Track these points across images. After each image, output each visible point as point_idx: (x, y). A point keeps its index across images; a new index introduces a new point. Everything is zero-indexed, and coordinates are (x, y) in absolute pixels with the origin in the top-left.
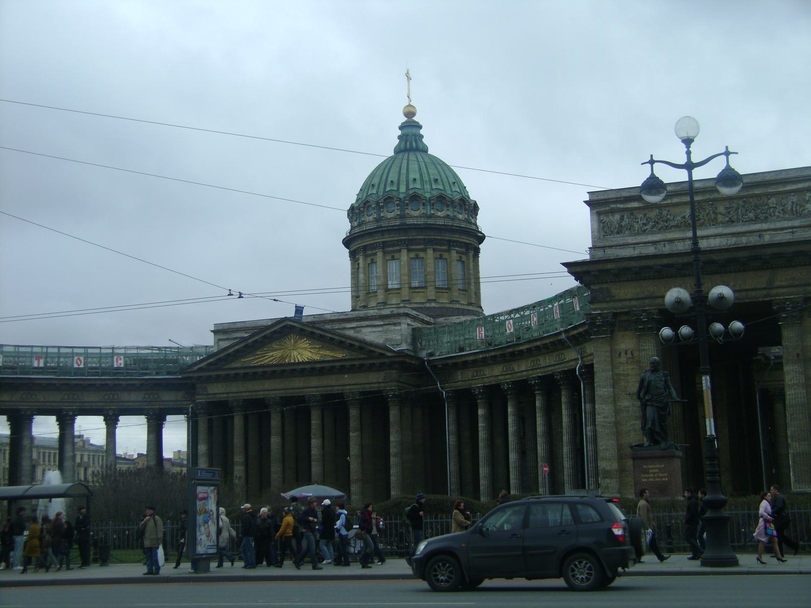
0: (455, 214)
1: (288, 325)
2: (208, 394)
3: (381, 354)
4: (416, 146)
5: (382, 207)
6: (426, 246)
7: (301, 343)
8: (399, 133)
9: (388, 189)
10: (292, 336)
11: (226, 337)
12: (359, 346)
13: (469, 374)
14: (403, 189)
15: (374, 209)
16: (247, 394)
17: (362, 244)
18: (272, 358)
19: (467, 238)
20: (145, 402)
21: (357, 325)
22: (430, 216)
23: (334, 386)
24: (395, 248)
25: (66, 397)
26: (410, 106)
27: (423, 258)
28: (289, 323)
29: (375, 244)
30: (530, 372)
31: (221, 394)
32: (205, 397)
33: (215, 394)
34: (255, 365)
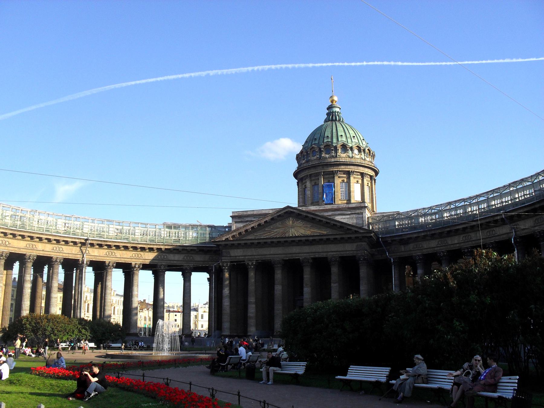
0: (366, 157)
1: (289, 211)
2: (231, 256)
3: (355, 231)
5: (322, 151)
8: (327, 111)
9: (325, 141)
10: (291, 219)
11: (240, 221)
13: (411, 246)
14: (335, 140)
16: (258, 257)
17: (309, 173)
18: (276, 233)
19: (371, 172)
20: (184, 261)
21: (332, 213)
23: (320, 252)
24: (331, 176)
25: (134, 255)
28: (290, 210)
29: (318, 173)
30: (462, 244)
31: (240, 256)
32: (229, 258)
33: (236, 256)
34: (264, 237)
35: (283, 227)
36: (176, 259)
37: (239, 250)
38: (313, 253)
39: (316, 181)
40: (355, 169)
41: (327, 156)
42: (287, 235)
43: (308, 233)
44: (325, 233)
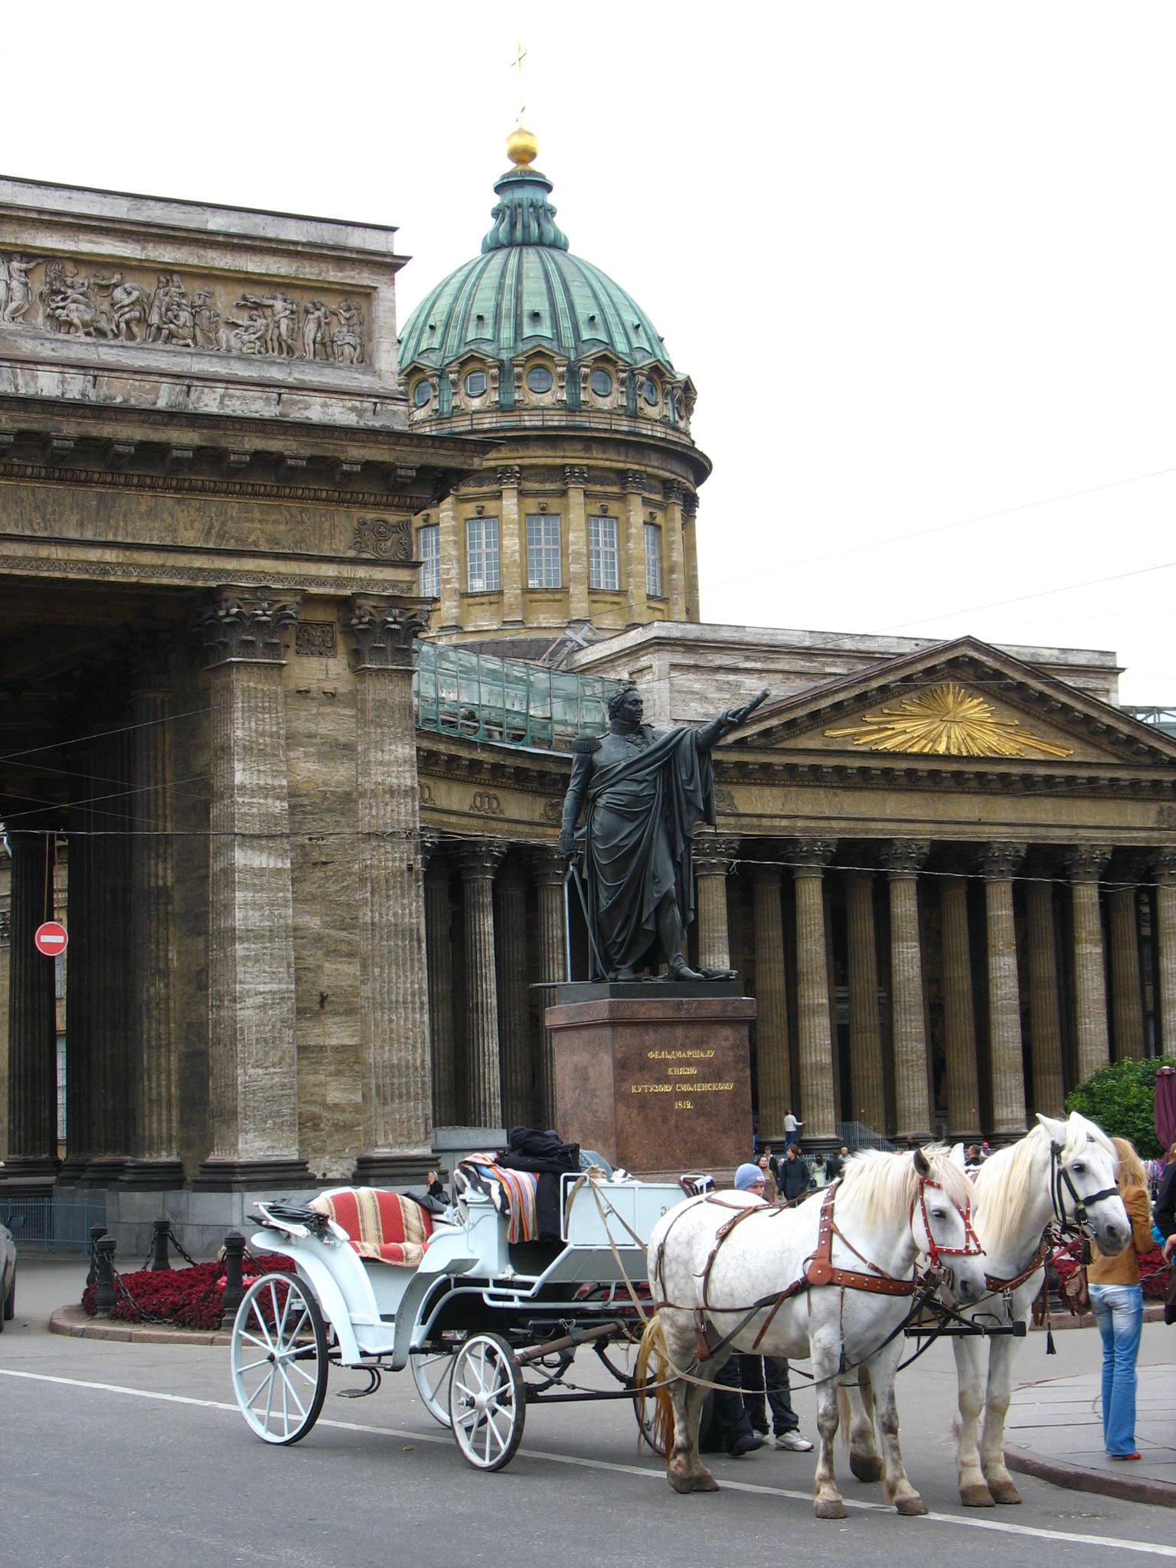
1: (964, 656)
4: (541, 234)
5: (585, 378)
6: (666, 496)
7: (972, 708)
9: (586, 335)
11: (692, 662)
12: (1128, 736)
14: (621, 346)
15: (561, 377)
16: (843, 824)
17: (518, 462)
22: (676, 429)
24: (610, 489)
26: (521, 132)
27: (658, 527)
32: (732, 820)
35: (928, 717)
36: (455, 807)
37: (767, 791)
38: (1028, 825)
39: (554, 504)
40: (683, 477)
41: (605, 404)
42: (941, 749)
43: (1008, 749)
44: (1062, 754)
